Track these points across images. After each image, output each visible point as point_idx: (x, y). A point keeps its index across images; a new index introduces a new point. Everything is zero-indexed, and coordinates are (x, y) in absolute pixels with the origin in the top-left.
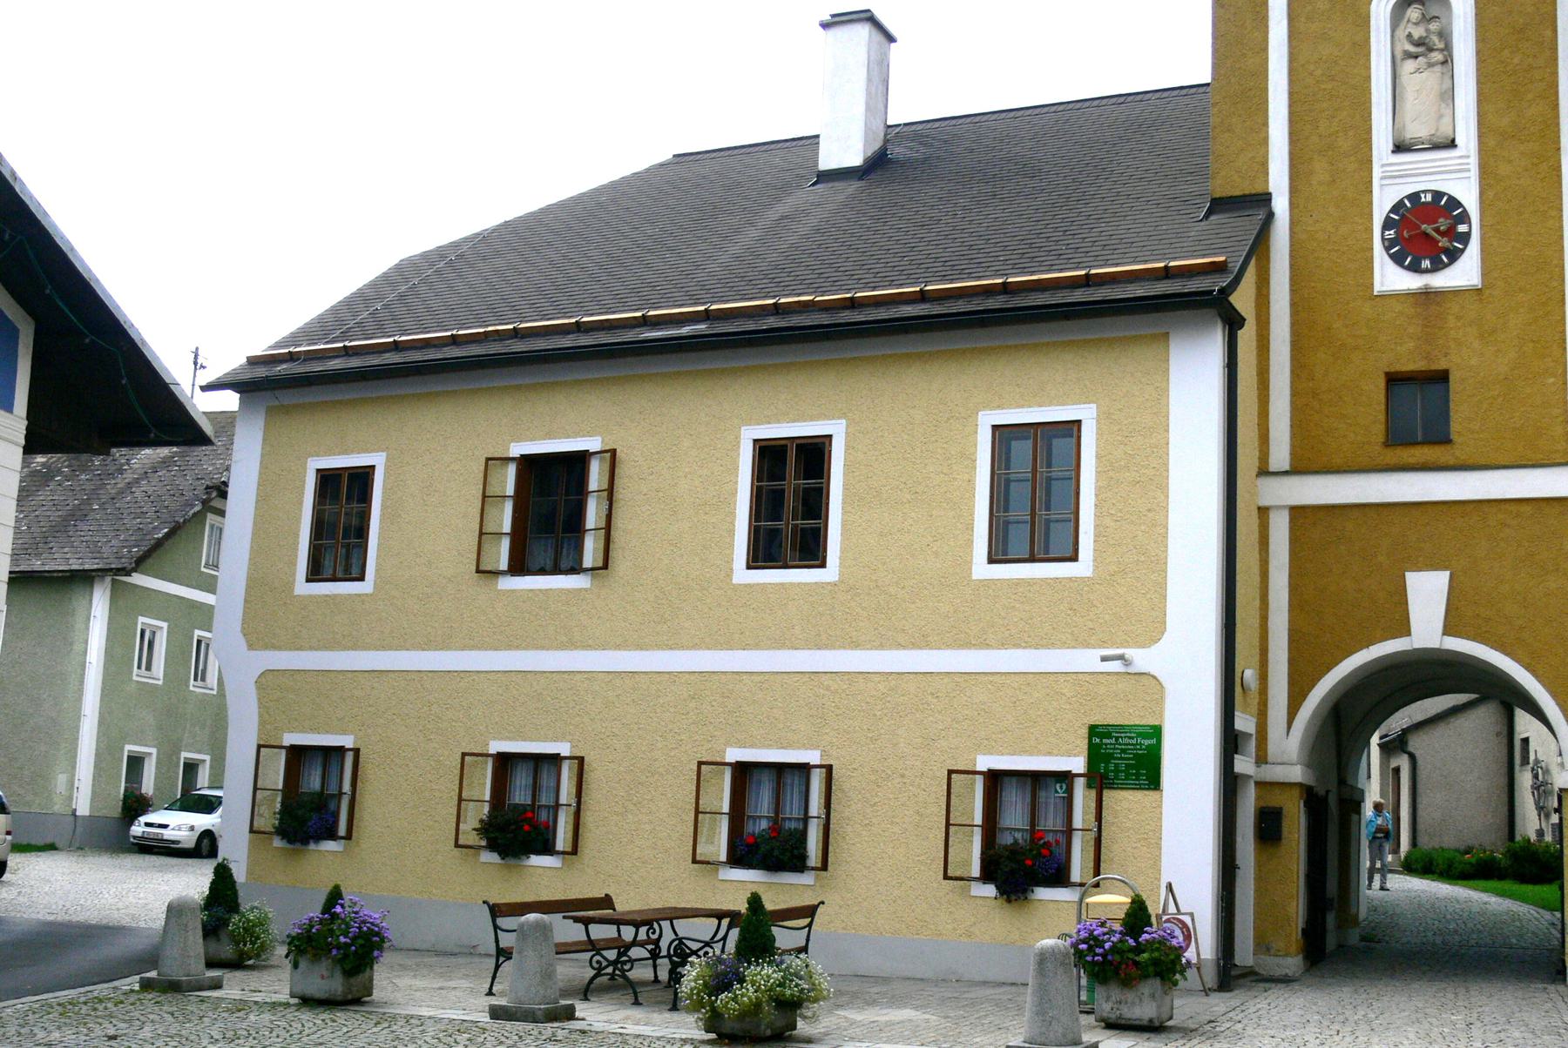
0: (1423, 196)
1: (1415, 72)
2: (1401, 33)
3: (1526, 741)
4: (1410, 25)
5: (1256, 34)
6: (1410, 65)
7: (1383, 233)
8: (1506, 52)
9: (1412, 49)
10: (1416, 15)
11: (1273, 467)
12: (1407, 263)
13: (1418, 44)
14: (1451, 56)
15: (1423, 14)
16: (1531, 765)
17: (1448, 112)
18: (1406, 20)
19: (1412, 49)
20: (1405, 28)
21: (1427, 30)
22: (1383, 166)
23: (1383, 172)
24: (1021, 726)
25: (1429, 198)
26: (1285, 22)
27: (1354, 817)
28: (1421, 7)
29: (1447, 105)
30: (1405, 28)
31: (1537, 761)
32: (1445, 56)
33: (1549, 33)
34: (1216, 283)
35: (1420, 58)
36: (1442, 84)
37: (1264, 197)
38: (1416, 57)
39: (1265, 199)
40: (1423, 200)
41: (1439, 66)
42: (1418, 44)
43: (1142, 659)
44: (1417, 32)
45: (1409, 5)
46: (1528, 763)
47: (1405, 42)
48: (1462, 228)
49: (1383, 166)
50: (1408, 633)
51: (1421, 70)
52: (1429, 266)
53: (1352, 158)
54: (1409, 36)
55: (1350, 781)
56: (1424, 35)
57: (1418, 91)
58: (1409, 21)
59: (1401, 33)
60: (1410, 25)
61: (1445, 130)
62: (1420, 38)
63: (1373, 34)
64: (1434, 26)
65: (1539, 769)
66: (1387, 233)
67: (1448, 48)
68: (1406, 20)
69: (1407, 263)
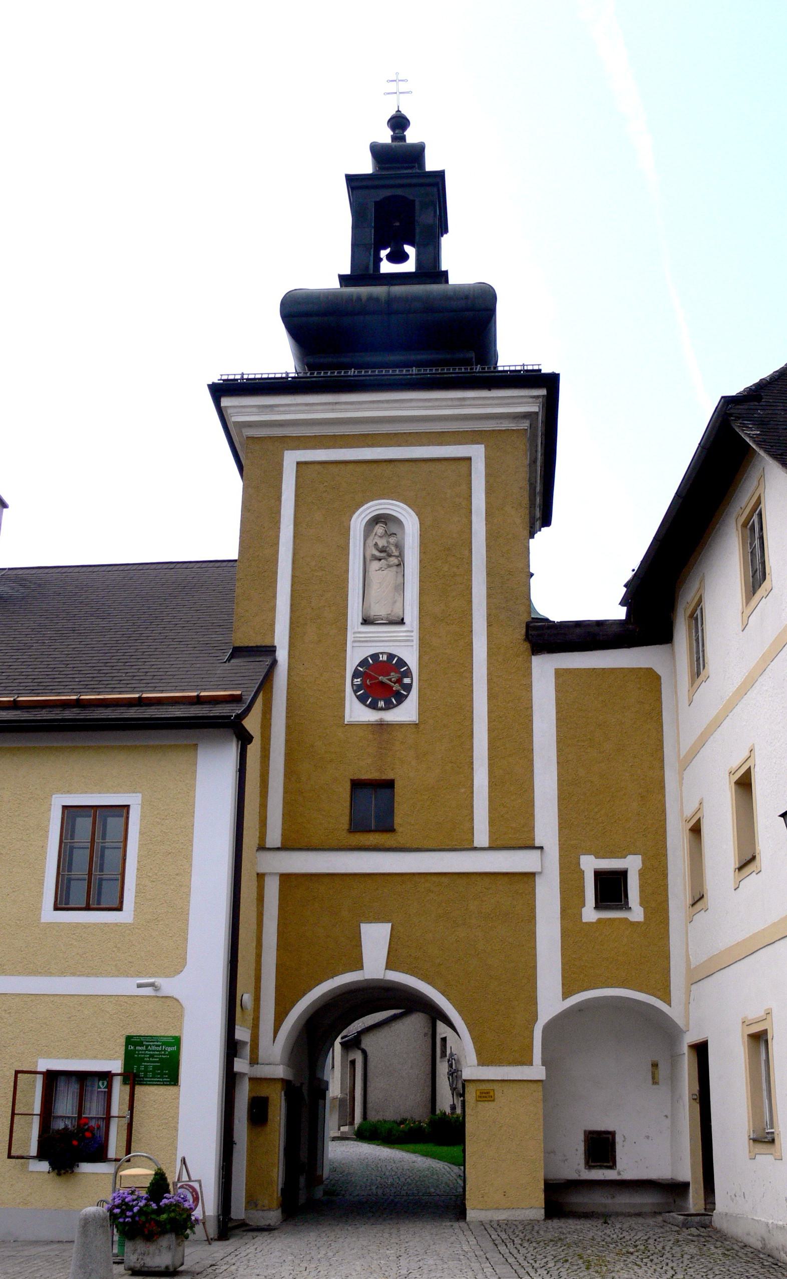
0: (381, 656)
1: (379, 570)
2: (371, 542)
3: (444, 1040)
4: (376, 537)
5: (270, 533)
6: (375, 565)
8: (439, 562)
9: (378, 554)
10: (381, 531)
11: (269, 845)
12: (368, 702)
13: (382, 551)
14: (403, 561)
15: (386, 531)
16: (448, 1057)
17: (400, 599)
18: (374, 534)
19: (378, 554)
20: (374, 539)
21: (388, 542)
22: (355, 633)
23: (354, 637)
24: (74, 1036)
25: (385, 658)
26: (292, 527)
27: (321, 1102)
28: (384, 526)
29: (399, 595)
30: (374, 539)
31: (451, 1055)
32: (399, 560)
33: (467, 552)
34: (233, 710)
35: (382, 561)
36: (396, 580)
37: (272, 649)
38: (380, 560)
39: (270, 650)
40: (381, 659)
41: (395, 567)
42: (382, 551)
43: (169, 986)
44: (382, 543)
45: (377, 524)
46: (446, 1056)
48: (407, 681)
49: (355, 633)
50: (360, 967)
51: (383, 569)
53: (334, 626)
54: (376, 544)
55: (319, 1075)
56: (386, 545)
57: (380, 583)
58: (376, 534)
59: (371, 542)
60: (376, 537)
61: (397, 612)
62: (383, 547)
63: (351, 541)
64: (392, 540)
65: (453, 1061)
66: (356, 680)
67: (401, 556)
68: (374, 534)
69: (368, 702)
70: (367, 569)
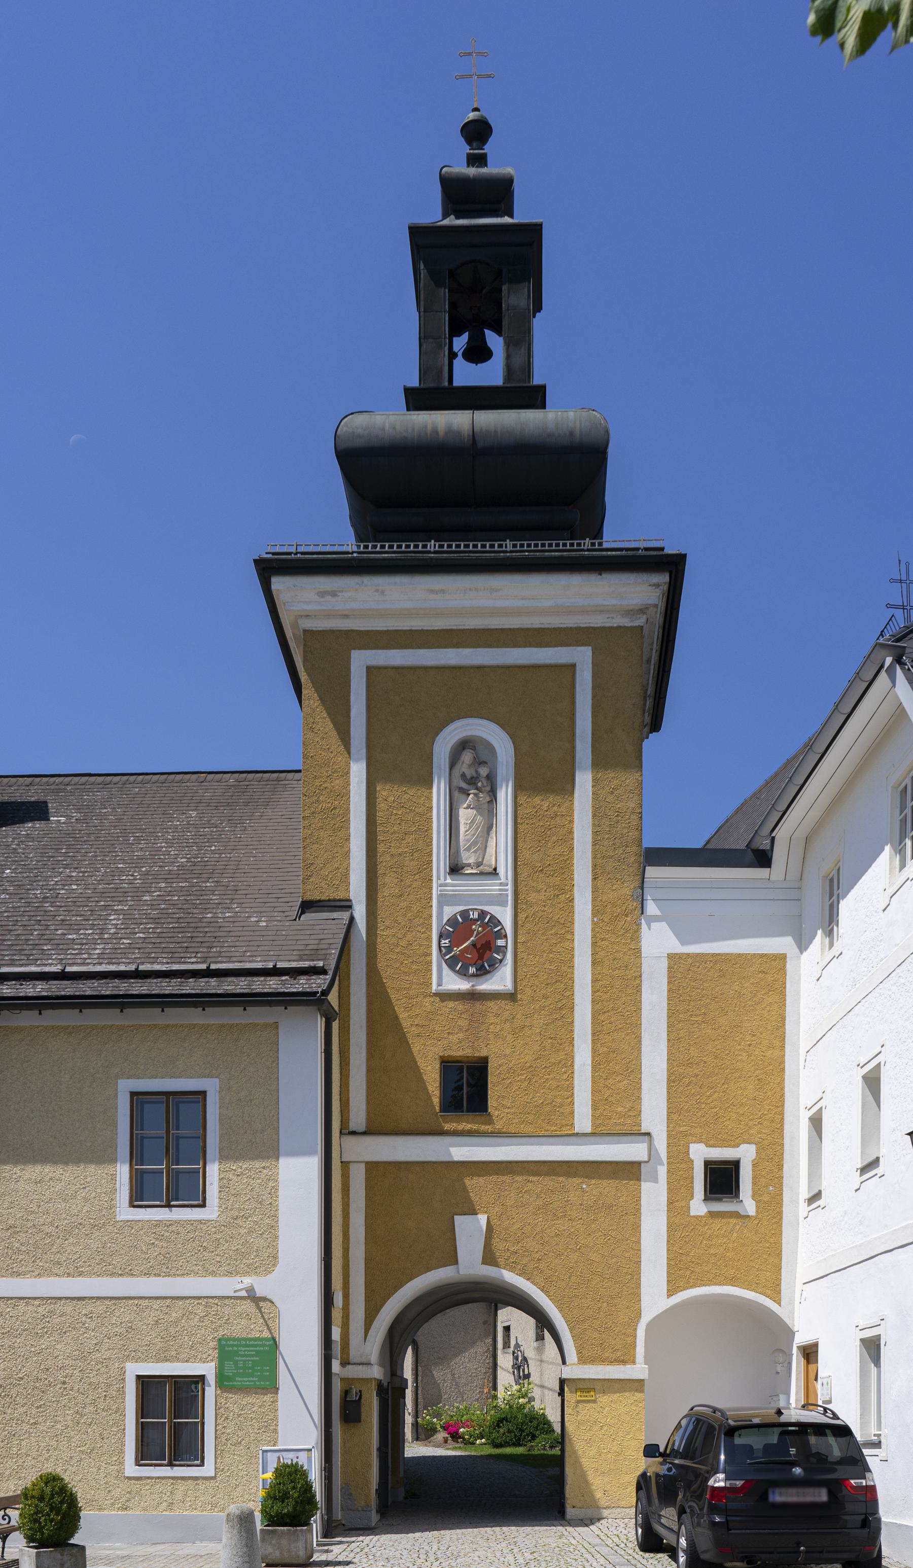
0: (471, 913)
3: (507, 1329)
7: (440, 942)
11: (353, 1126)
12: (458, 968)
16: (512, 1349)
22: (441, 885)
23: (441, 891)
24: (162, 1340)
25: (476, 916)
27: (402, 1400)
28: (473, 752)
31: (517, 1346)
34: (317, 983)
37: (348, 904)
39: (345, 905)
40: (471, 916)
43: (263, 1285)
44: (469, 773)
46: (509, 1347)
47: (461, 781)
48: (500, 942)
49: (441, 885)
50: (455, 1261)
52: (471, 968)
53: (417, 877)
55: (399, 1373)
59: (457, 772)
65: (519, 1352)
66: (443, 941)
69: (458, 968)
70: (454, 807)
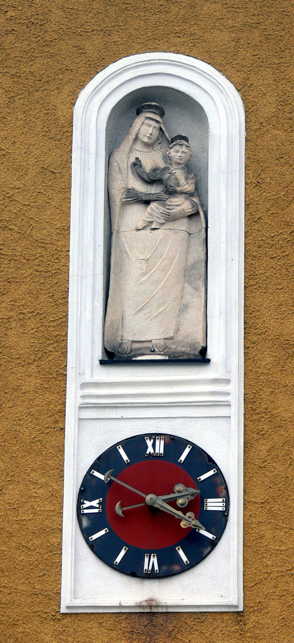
0: (149, 443)
1: (144, 228)
4: (138, 146)
7: (79, 504)
10: (150, 130)
12: (118, 559)
14: (205, 206)
18: (131, 137)
20: (131, 150)
21: (167, 158)
22: (84, 385)
23: (83, 397)
28: (158, 118)
30: (131, 150)
32: (194, 205)
36: (188, 252)
38: (147, 203)
40: (150, 450)
45: (138, 112)
47: (131, 175)
49: (84, 385)
52: (156, 568)
53: (33, 368)
54: (137, 164)
56: (162, 165)
58: (136, 138)
60: (138, 146)
62: (155, 170)
63: (75, 155)
66: (87, 504)
68: (131, 137)
69: (118, 560)
70: (115, 227)
